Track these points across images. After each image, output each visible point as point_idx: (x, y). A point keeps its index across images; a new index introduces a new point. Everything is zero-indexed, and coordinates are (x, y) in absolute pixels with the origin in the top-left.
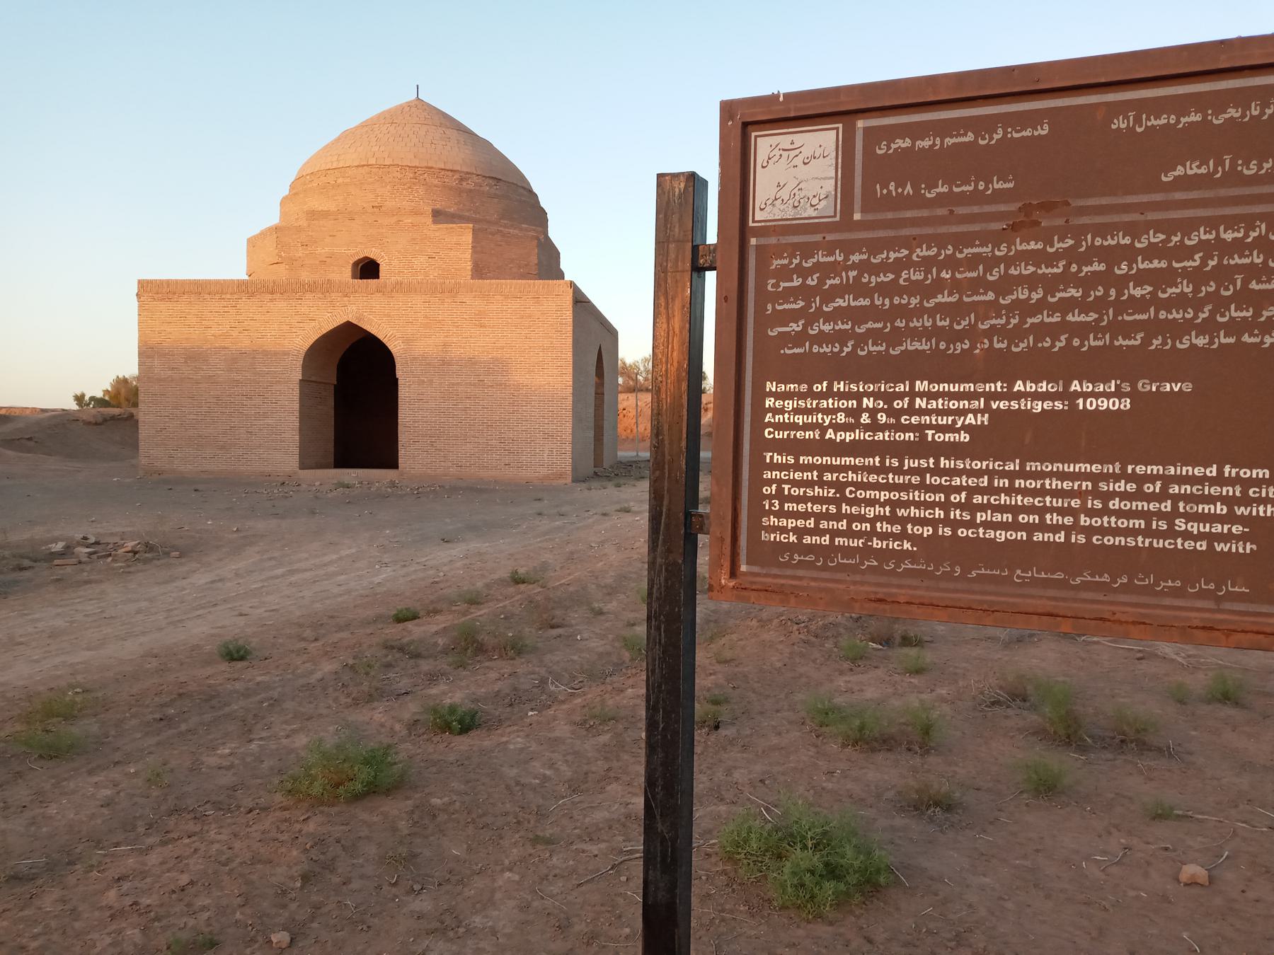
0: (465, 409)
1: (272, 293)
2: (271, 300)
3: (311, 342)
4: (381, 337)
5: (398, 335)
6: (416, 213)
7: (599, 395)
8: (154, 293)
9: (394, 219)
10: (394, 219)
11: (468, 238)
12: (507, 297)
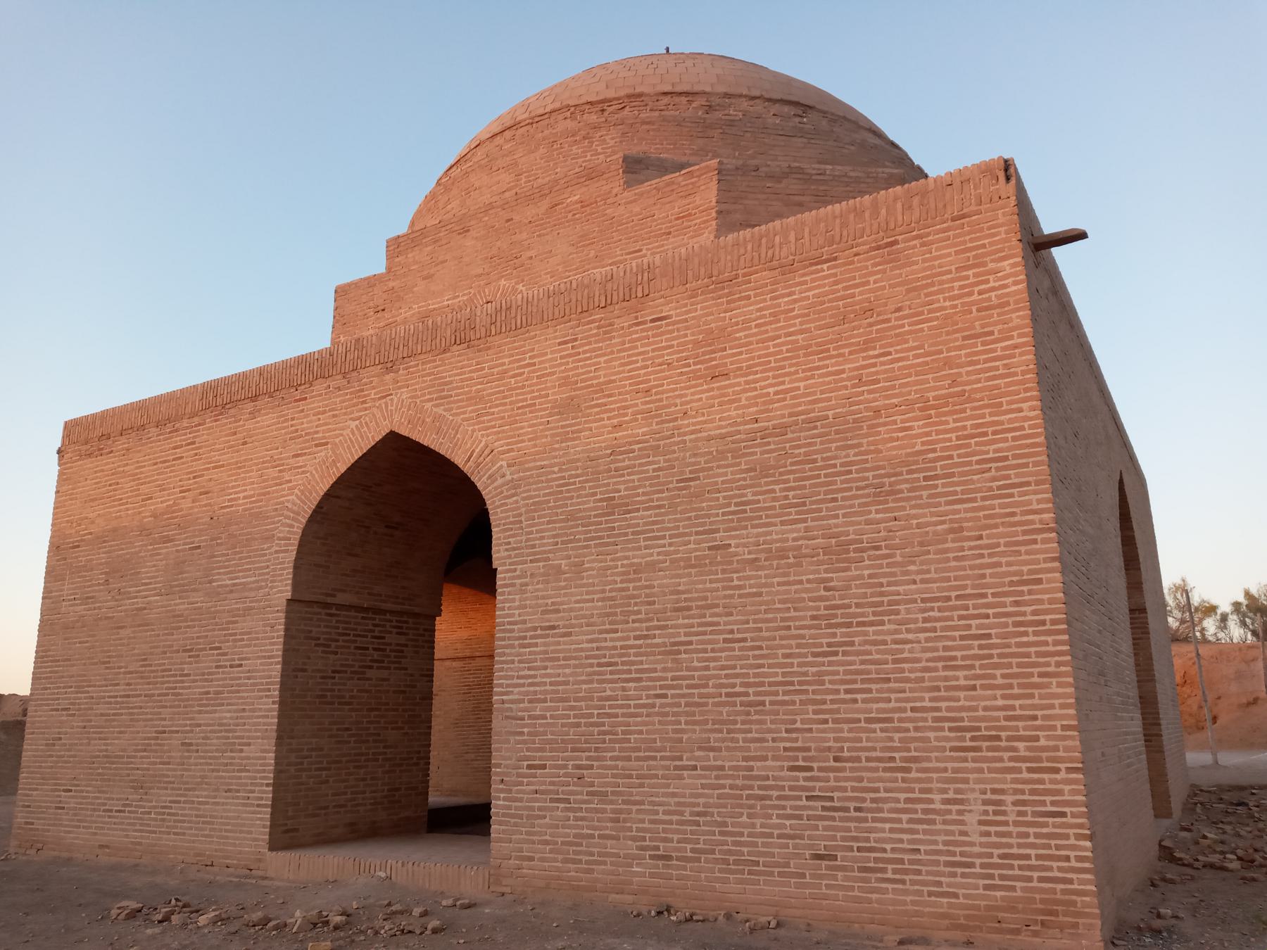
0: (673, 650)
1: (254, 398)
2: (253, 415)
4: (459, 460)
5: (499, 445)
6: (591, 175)
7: (1138, 612)
8: (86, 440)
9: (545, 204)
10: (545, 204)
11: (708, 194)
12: (787, 268)
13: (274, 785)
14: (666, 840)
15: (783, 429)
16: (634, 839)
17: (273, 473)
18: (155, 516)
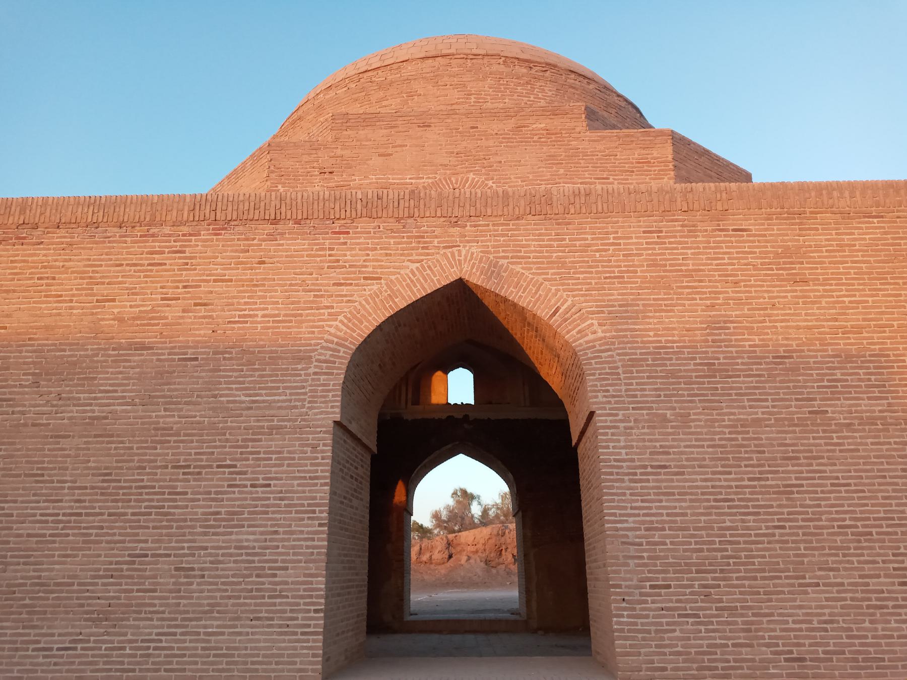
0: (787, 491)
1: (275, 221)
2: (271, 237)
3: (367, 328)
9: (511, 123)
10: (511, 123)
12: (846, 215)
13: (325, 611)
14: (798, 645)
15: (858, 330)
16: (768, 645)
17: (310, 296)
18: (121, 320)
